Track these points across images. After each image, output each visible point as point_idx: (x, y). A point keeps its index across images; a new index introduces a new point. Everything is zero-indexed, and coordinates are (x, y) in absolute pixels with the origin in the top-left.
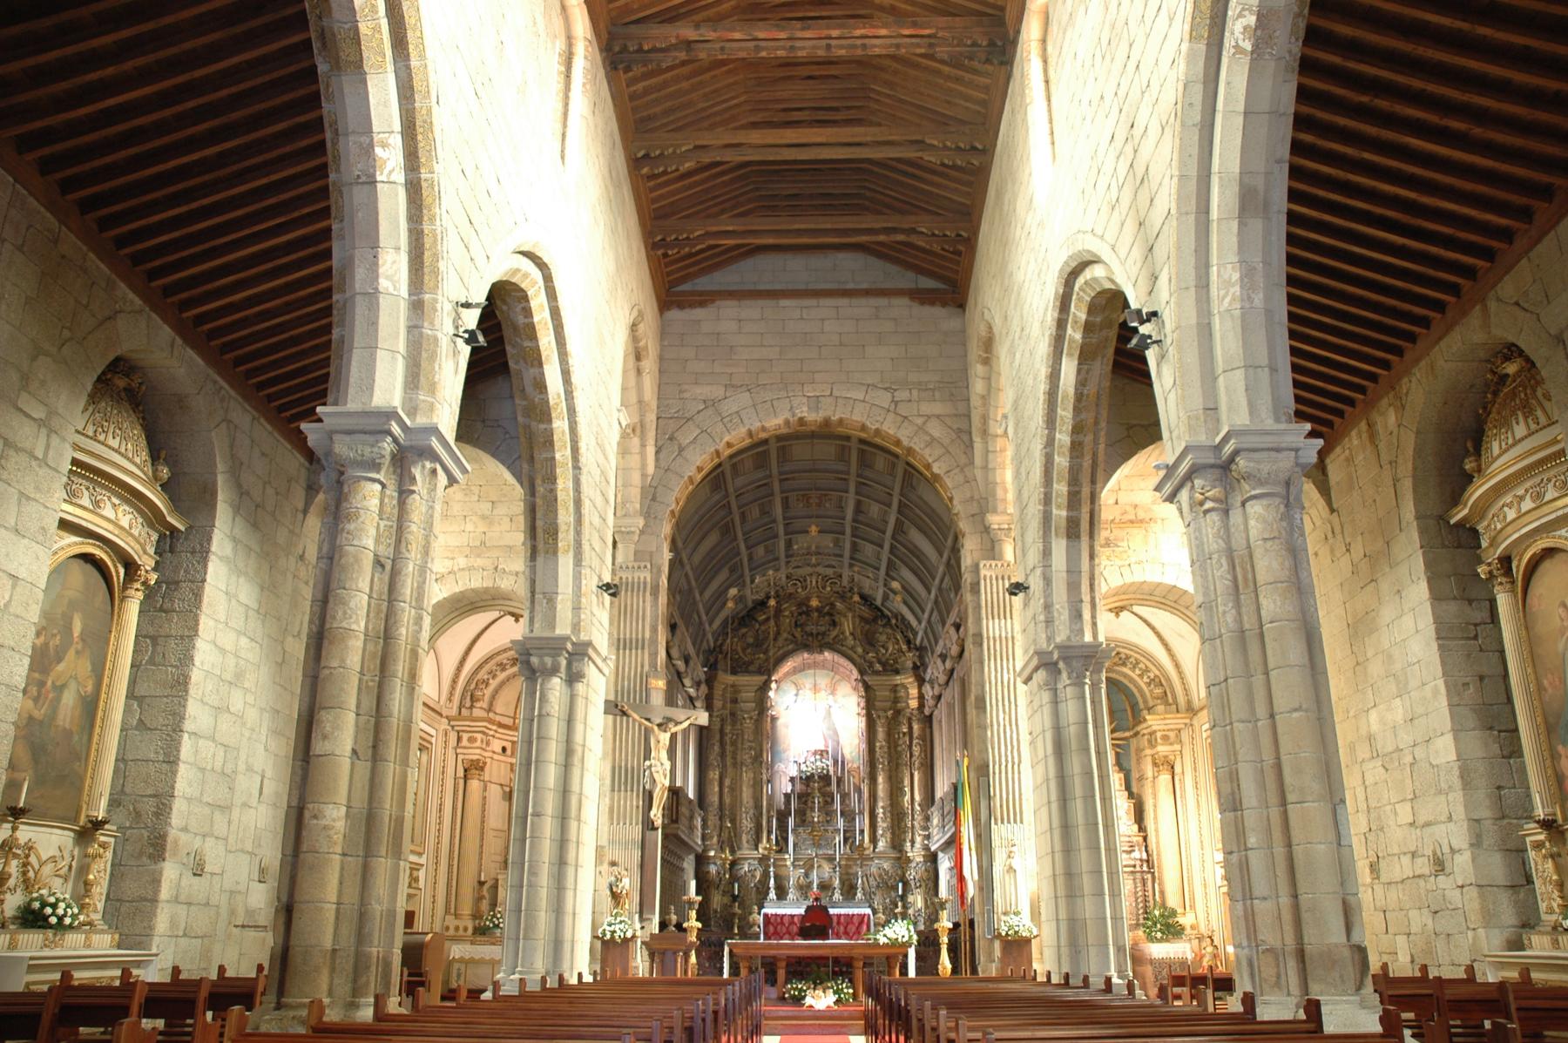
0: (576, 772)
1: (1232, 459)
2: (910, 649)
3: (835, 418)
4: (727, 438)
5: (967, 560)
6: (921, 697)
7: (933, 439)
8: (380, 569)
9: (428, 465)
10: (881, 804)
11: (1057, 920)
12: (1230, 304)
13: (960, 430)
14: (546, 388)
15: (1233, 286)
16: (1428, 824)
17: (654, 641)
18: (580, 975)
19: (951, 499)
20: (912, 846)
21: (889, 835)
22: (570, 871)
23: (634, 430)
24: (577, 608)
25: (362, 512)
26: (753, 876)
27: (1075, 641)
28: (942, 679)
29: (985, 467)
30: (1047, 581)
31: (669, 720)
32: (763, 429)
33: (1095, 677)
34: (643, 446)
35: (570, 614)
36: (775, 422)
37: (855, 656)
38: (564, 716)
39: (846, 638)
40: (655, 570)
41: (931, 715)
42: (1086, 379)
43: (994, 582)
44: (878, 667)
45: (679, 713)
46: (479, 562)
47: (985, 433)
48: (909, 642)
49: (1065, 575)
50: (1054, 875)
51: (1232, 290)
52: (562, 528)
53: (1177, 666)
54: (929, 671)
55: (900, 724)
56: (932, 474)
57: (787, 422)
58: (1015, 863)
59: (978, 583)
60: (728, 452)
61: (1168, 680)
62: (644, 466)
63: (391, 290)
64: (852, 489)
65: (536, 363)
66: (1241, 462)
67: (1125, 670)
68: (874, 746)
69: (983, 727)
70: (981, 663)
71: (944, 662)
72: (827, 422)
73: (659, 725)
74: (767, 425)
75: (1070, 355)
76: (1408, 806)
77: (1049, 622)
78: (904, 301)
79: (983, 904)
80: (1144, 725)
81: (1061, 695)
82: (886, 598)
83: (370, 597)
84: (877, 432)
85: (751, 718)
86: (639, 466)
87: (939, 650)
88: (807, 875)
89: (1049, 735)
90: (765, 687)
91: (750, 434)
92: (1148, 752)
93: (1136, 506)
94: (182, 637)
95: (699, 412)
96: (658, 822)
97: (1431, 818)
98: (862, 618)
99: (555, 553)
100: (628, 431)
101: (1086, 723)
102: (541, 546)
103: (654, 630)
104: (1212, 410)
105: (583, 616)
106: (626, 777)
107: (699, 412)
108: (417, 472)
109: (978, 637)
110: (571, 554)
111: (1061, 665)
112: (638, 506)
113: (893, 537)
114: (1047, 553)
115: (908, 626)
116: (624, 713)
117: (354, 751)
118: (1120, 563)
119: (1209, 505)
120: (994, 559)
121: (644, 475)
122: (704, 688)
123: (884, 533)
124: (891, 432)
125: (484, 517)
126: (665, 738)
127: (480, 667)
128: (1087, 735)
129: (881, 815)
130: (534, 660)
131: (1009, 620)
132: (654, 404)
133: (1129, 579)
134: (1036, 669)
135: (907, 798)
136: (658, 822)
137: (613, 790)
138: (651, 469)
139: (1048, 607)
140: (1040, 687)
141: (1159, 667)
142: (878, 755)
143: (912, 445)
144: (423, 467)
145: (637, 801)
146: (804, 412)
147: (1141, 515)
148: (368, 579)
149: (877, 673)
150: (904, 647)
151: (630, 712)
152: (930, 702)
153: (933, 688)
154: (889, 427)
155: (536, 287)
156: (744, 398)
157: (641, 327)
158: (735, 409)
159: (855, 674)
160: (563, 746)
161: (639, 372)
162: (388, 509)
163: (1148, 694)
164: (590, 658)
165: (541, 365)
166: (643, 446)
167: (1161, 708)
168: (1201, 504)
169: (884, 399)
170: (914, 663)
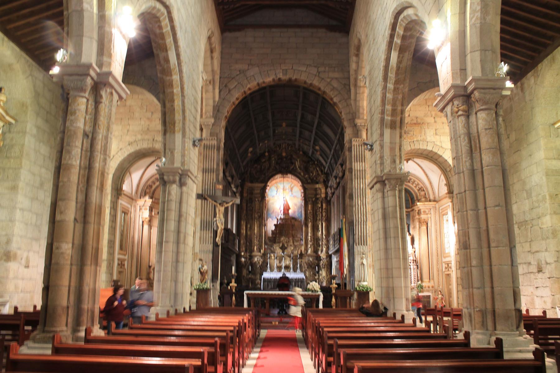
0: (183, 224)
1: (472, 92)
2: (322, 174)
3: (294, 78)
4: (249, 86)
5: (347, 138)
6: (326, 193)
7: (334, 88)
8: (86, 137)
9: (108, 90)
10: (309, 235)
11: (382, 287)
12: (475, 21)
13: (345, 85)
14: (169, 61)
15: (477, 12)
16: (537, 252)
17: (218, 169)
18: (184, 309)
19: (341, 113)
22: (180, 265)
23: (210, 82)
24: (183, 156)
25: (77, 111)
26: (259, 263)
27: (392, 172)
28: (335, 186)
29: (355, 100)
30: (382, 147)
31: (224, 202)
32: (264, 82)
33: (400, 187)
34: (214, 89)
35: (180, 158)
36: (269, 80)
37: (300, 176)
38: (178, 200)
39: (296, 169)
40: (218, 140)
42: (401, 61)
43: (358, 147)
44: (309, 181)
45: (228, 199)
46: (146, 137)
47: (356, 85)
48: (322, 171)
49: (389, 144)
50: (381, 269)
51: (476, 14)
52: (177, 122)
53: (431, 183)
54: (330, 183)
55: (317, 203)
56: (333, 102)
57: (274, 80)
58: (365, 262)
59: (351, 147)
60: (249, 92)
61: (427, 189)
62: (214, 98)
63: (89, 8)
64: (300, 108)
65: (165, 50)
66: (476, 93)
67: (410, 184)
69: (352, 206)
70: (352, 180)
71: (336, 179)
72: (290, 80)
73: (220, 204)
74: (266, 81)
75: (395, 50)
76: (528, 244)
77: (382, 164)
78: (324, 30)
79: (350, 277)
80: (416, 207)
81: (386, 195)
82: (313, 153)
83: (82, 150)
84: (311, 84)
86: (212, 97)
87: (334, 174)
88: (280, 262)
89: (380, 211)
90: (264, 190)
91: (258, 84)
92: (417, 217)
93: (417, 118)
94: (15, 169)
95: (237, 75)
96: (219, 243)
97: (538, 249)
99: (174, 132)
100: (208, 82)
101: (396, 206)
102: (168, 129)
103: (218, 165)
104: (463, 70)
105: (186, 159)
106: (206, 225)
107: (237, 75)
108: (103, 93)
109: (351, 170)
110: (181, 133)
111: (386, 182)
112: (212, 114)
113: (317, 128)
114: (382, 135)
115: (322, 164)
116: (205, 199)
117: (75, 219)
118: (410, 141)
119: (460, 113)
120: (358, 137)
121: (214, 101)
122: (240, 189)
123: (313, 126)
124: (317, 84)
125: (148, 119)
126: (222, 209)
127: (149, 180)
128: (396, 212)
129: (309, 239)
130: (166, 178)
131: (364, 163)
132: (218, 72)
133: (413, 147)
134: (376, 183)
136: (219, 243)
137: (201, 230)
138: (217, 98)
139: (382, 158)
140: (377, 191)
141: (423, 183)
142: (309, 216)
143: (325, 90)
144: (106, 91)
145: (210, 235)
146: (281, 76)
147: (419, 121)
148: (81, 141)
149: (308, 183)
150: (320, 173)
151: (208, 198)
152: (330, 195)
153: (331, 190)
154: (316, 82)
155: (164, 16)
156: (256, 69)
157: (213, 39)
158: (252, 74)
160: (177, 213)
161: (212, 58)
162: (90, 110)
163: (418, 194)
164: (189, 176)
165: (167, 51)
166: (214, 89)
167: (423, 199)
168: (457, 112)
169: (314, 71)
170: (324, 180)
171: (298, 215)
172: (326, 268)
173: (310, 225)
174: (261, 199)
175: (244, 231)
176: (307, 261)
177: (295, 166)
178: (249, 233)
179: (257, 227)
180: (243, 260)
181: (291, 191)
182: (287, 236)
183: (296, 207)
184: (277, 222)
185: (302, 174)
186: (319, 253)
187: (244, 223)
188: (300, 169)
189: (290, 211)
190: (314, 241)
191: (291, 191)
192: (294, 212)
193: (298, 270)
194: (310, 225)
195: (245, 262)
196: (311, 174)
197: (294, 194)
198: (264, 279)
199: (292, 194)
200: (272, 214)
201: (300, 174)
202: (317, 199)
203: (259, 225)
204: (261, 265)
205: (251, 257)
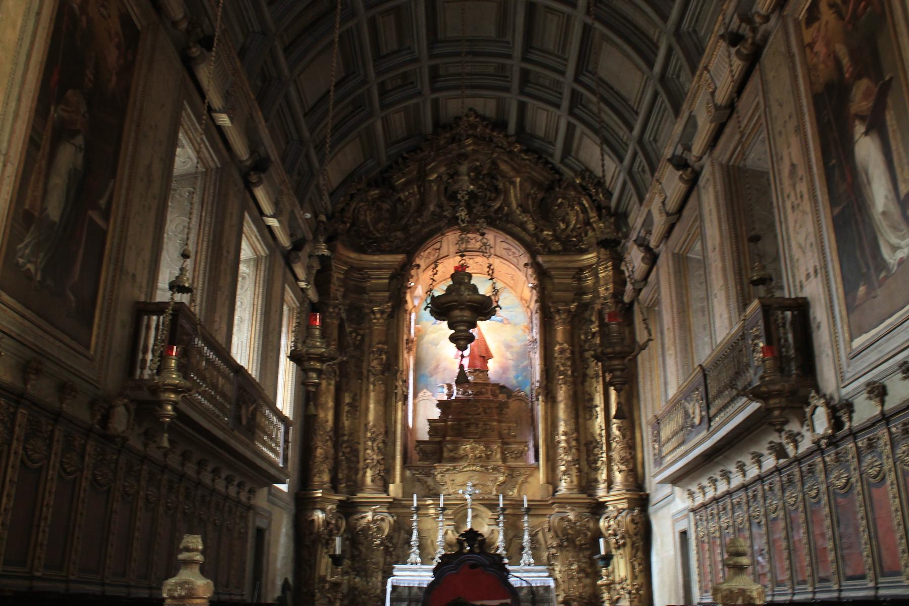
10: (562, 428)
20: (609, 488)
21: (574, 472)
26: (379, 529)
37: (523, 234)
39: (511, 213)
41: (631, 304)
44: (557, 245)
48: (599, 208)
68: (553, 351)
85: (382, 312)
98: (534, 182)
129: (563, 444)
135: (600, 421)
142: (557, 363)
159: (525, 259)
171: (517, 377)
172: (628, 549)
173: (562, 394)
174: (393, 307)
175: (327, 416)
176: (555, 520)
177: (507, 202)
178: (347, 423)
179: (377, 402)
180: (319, 516)
182: (482, 437)
183: (509, 355)
184: (450, 395)
185: (531, 227)
186: (601, 493)
187: (328, 389)
188: (525, 211)
189: (492, 365)
190: (578, 450)
192: (505, 370)
193: (526, 557)
194: (562, 394)
195: (327, 523)
196: (562, 226)
198: (394, 588)
200: (431, 376)
201: (522, 225)
202: (585, 307)
203: (382, 396)
204: (390, 537)
205: (348, 509)
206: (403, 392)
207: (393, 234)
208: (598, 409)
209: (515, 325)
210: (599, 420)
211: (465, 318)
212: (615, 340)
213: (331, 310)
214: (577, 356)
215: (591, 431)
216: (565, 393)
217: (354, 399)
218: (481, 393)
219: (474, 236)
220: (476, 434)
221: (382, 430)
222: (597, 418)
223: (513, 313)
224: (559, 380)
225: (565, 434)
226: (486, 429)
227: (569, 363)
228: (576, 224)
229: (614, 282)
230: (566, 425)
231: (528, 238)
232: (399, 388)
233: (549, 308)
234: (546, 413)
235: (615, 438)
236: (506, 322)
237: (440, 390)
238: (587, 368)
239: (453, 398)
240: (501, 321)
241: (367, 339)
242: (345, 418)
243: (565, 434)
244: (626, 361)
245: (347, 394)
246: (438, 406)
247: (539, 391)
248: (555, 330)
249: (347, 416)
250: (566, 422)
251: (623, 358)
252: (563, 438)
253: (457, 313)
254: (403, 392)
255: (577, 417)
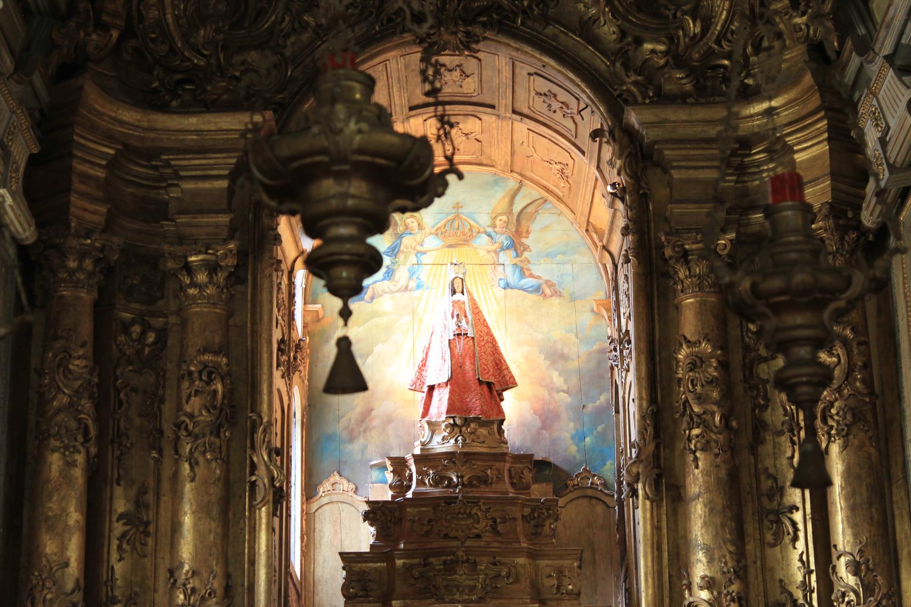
10: (700, 569)
37: (588, 53)
68: (671, 363)
85: (212, 268)
142: (683, 393)
159: (594, 120)
171: (579, 437)
174: (242, 255)
178: (119, 568)
179: (202, 510)
181: (516, 244)
183: (557, 380)
184: (400, 487)
185: (608, 31)
187: (65, 476)
191: (516, 244)
196: (694, 28)
197: (542, 270)
199: (523, 273)
200: (352, 440)
203: (215, 491)
206: (272, 479)
207: (237, 59)
208: (798, 516)
209: (573, 299)
210: (801, 545)
211: (350, 202)
212: (793, 256)
213: (73, 264)
214: (738, 375)
215: (779, 575)
216: (706, 473)
217: (139, 503)
218: (484, 481)
219: (456, 60)
220: (473, 588)
221: (217, 584)
222: (795, 538)
223: (568, 267)
224: (689, 440)
225: (710, 584)
226: (498, 576)
227: (715, 395)
228: (729, 20)
229: (834, 175)
230: (710, 561)
231: (601, 63)
232: (262, 470)
233: (661, 247)
234: (656, 529)
235: (844, 595)
236: (548, 291)
237: (375, 474)
238: (764, 408)
239: (409, 495)
240: (537, 290)
241: (172, 341)
242: (115, 556)
243: (710, 584)
244: (826, 315)
245: (118, 491)
246: (367, 516)
247: (634, 470)
248: (677, 308)
249: (120, 547)
250: (708, 550)
251: (818, 306)
252: (704, 595)
253: (328, 186)
254: (272, 479)
255: (740, 537)
